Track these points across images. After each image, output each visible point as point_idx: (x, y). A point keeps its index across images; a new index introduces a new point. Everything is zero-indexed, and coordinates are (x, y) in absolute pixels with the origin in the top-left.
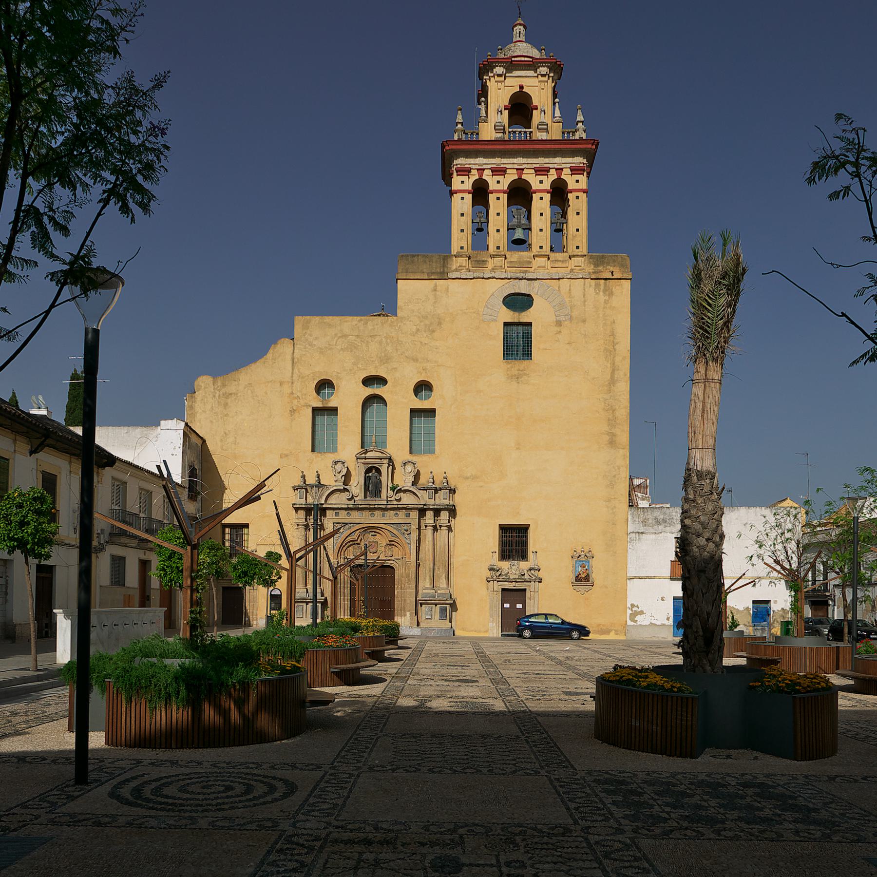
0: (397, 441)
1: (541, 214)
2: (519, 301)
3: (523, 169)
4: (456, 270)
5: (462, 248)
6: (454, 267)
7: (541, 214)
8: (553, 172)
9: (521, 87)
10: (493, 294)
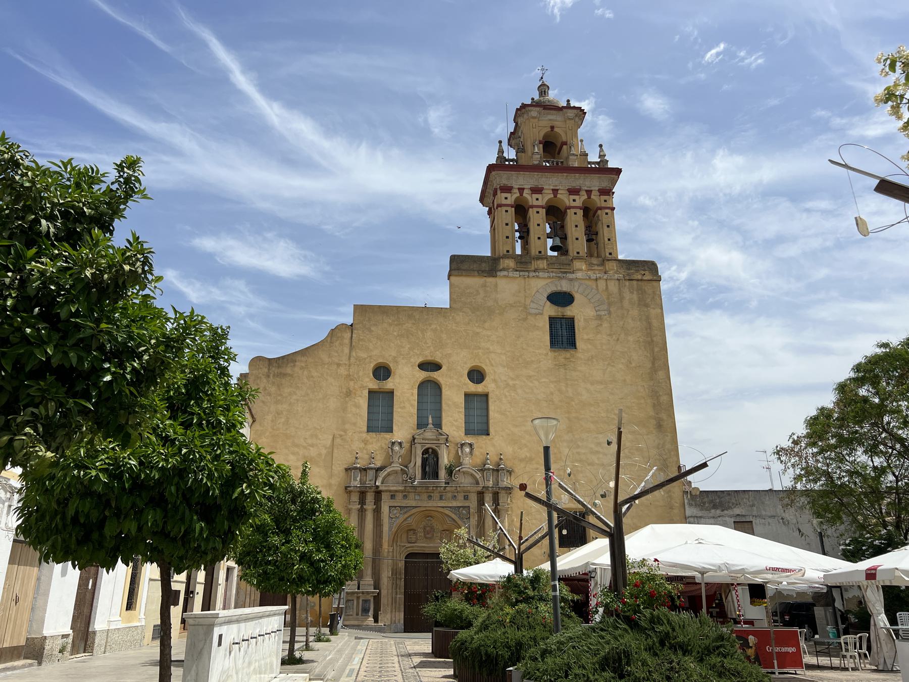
0: (453, 420)
1: (576, 226)
2: (561, 299)
4: (504, 269)
5: (508, 251)
6: (501, 267)
7: (576, 226)
9: (552, 128)
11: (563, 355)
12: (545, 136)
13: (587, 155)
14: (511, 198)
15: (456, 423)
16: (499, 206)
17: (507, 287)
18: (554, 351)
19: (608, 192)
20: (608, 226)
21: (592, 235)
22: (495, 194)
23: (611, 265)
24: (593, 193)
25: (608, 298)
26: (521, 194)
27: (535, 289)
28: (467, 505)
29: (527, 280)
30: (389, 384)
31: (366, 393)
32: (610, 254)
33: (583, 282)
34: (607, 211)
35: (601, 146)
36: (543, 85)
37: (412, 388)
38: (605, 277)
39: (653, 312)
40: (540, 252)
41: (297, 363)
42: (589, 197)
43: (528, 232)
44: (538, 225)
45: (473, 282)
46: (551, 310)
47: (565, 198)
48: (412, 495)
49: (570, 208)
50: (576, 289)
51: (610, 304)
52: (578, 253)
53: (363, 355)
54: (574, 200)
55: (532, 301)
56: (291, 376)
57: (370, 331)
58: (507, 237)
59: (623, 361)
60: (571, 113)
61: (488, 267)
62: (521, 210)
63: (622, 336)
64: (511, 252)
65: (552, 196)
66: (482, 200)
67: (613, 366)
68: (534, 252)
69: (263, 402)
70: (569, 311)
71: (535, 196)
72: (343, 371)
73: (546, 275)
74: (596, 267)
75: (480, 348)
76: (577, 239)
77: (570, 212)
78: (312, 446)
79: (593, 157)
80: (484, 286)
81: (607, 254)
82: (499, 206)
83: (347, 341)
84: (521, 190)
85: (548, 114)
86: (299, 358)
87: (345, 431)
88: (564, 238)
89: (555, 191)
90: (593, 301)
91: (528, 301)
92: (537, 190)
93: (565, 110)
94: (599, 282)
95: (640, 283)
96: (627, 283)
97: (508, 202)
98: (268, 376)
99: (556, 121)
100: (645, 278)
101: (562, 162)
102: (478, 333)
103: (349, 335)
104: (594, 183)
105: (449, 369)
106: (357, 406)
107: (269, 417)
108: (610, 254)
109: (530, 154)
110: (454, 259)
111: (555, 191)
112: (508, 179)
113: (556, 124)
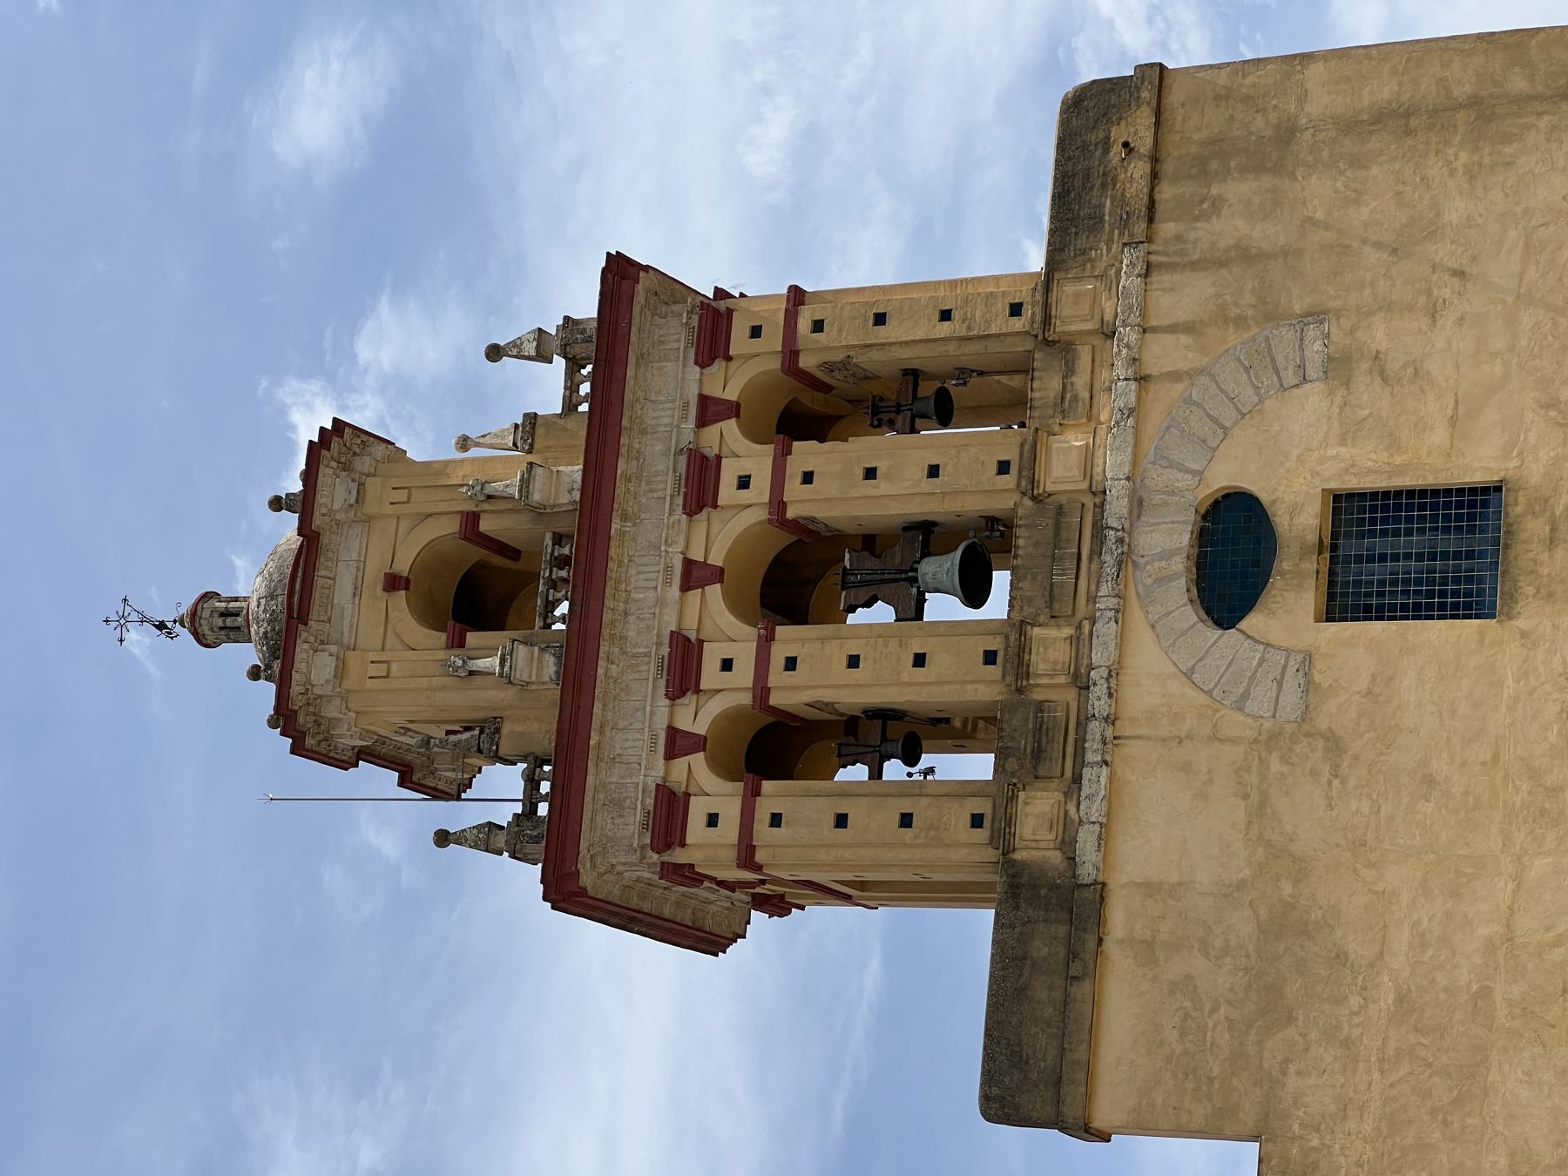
1: (871, 473)
2: (1232, 556)
3: (688, 564)
4: (1067, 845)
5: (977, 821)
6: (1055, 857)
7: (871, 473)
8: (710, 439)
9: (393, 582)
10: (1188, 675)
11: (1533, 551)
12: (429, 616)
13: (532, 419)
14: (714, 794)
16: (746, 854)
17: (1159, 833)
18: (1512, 597)
19: (714, 321)
20: (880, 319)
21: (917, 399)
22: (687, 875)
23: (1072, 314)
24: (714, 390)
25: (1241, 322)
26: (697, 743)
27: (1178, 687)
29: (1124, 728)
32: (1016, 310)
33: (1149, 446)
34: (804, 325)
35: (494, 353)
36: (193, 621)
38: (1129, 335)
39: (1321, 100)
40: (990, 657)
42: (732, 410)
43: (884, 716)
44: (853, 662)
45: (1126, 1015)
46: (1289, 611)
47: (732, 529)
49: (778, 504)
50: (1184, 481)
51: (1272, 315)
52: (1003, 468)
54: (744, 483)
55: (1239, 706)
58: (906, 820)
60: (335, 493)
61: (1049, 926)
62: (778, 746)
63: (1441, 251)
64: (983, 806)
65: (715, 590)
66: (712, 942)
68: (982, 688)
70: (1299, 515)
71: (710, 675)
73: (1106, 629)
74: (1080, 381)
75: (1485, 993)
76: (934, 471)
79: (544, 387)
80: (1147, 949)
81: (1018, 324)
82: (746, 854)
84: (678, 743)
88: (926, 535)
89: (694, 575)
90: (1248, 397)
91: (1236, 724)
92: (683, 665)
93: (318, 521)
94: (1151, 366)
95: (1168, 167)
96: (1167, 229)
97: (731, 812)
100: (1145, 143)
101: (558, 539)
102: (1400, 999)
104: (666, 384)
108: (1016, 310)
109: (509, 694)
110: (1007, 1098)
111: (694, 575)
112: (618, 804)
113: (375, 570)
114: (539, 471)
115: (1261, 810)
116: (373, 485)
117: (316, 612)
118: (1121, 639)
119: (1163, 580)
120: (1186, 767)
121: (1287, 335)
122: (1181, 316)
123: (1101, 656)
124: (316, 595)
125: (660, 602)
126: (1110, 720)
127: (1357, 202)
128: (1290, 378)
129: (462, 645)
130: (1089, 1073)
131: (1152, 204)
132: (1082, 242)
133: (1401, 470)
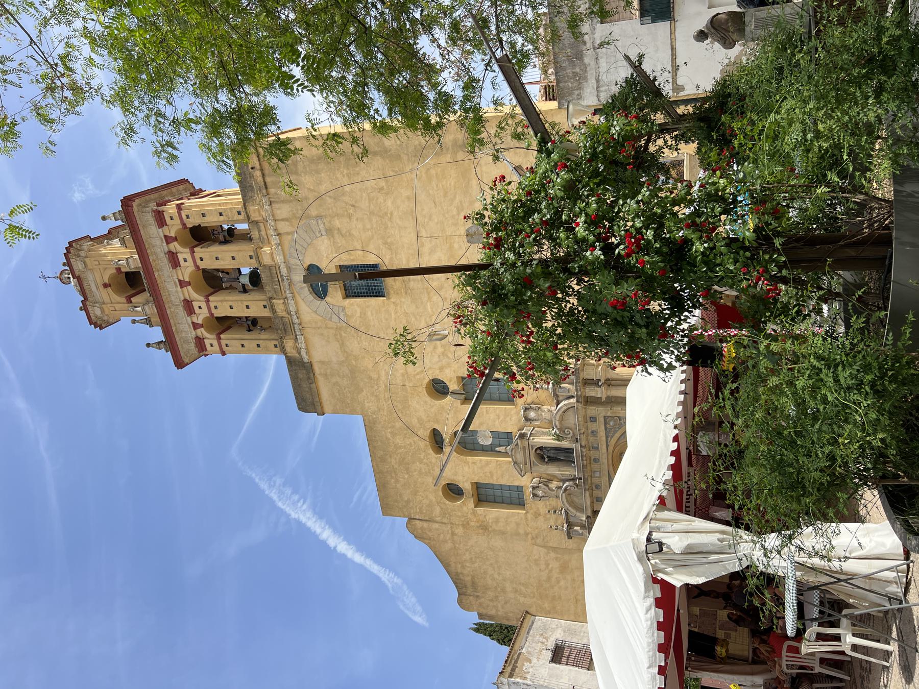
3: (180, 281)
4: (300, 353)
6: (297, 355)
9: (106, 286)
10: (316, 312)
12: (119, 291)
15: (502, 418)
26: (201, 326)
27: (314, 315)
28: (602, 420)
30: (466, 486)
31: (480, 510)
33: (287, 252)
34: (184, 217)
37: (466, 463)
41: (459, 571)
42: (175, 239)
46: (335, 294)
47: (187, 270)
48: (595, 480)
52: (251, 257)
53: (437, 510)
56: (473, 577)
57: (408, 501)
59: (381, 200)
61: (301, 372)
63: (346, 199)
64: (276, 343)
67: (392, 214)
69: (506, 603)
72: (460, 531)
73: (291, 302)
74: (263, 233)
77: (202, 265)
78: (547, 565)
80: (325, 375)
83: (425, 525)
85: (91, 291)
86: (453, 569)
87: (527, 534)
92: (188, 306)
93: (77, 274)
94: (281, 231)
98: (477, 596)
99: (95, 281)
100: (258, 166)
103: (417, 522)
105: (437, 422)
106: (497, 520)
107: (522, 599)
108: (239, 213)
112: (187, 342)
113: (100, 283)
114: (130, 260)
115: (342, 345)
116: (87, 260)
117: (89, 295)
118: (296, 304)
119: (301, 288)
120: (322, 335)
121: (314, 222)
122: (284, 216)
123: (292, 308)
124: (87, 291)
125: (177, 292)
126: (300, 324)
127: (320, 184)
128: (319, 235)
129: (131, 302)
130: (320, 402)
131: (265, 183)
132: (250, 194)
133: (353, 260)
